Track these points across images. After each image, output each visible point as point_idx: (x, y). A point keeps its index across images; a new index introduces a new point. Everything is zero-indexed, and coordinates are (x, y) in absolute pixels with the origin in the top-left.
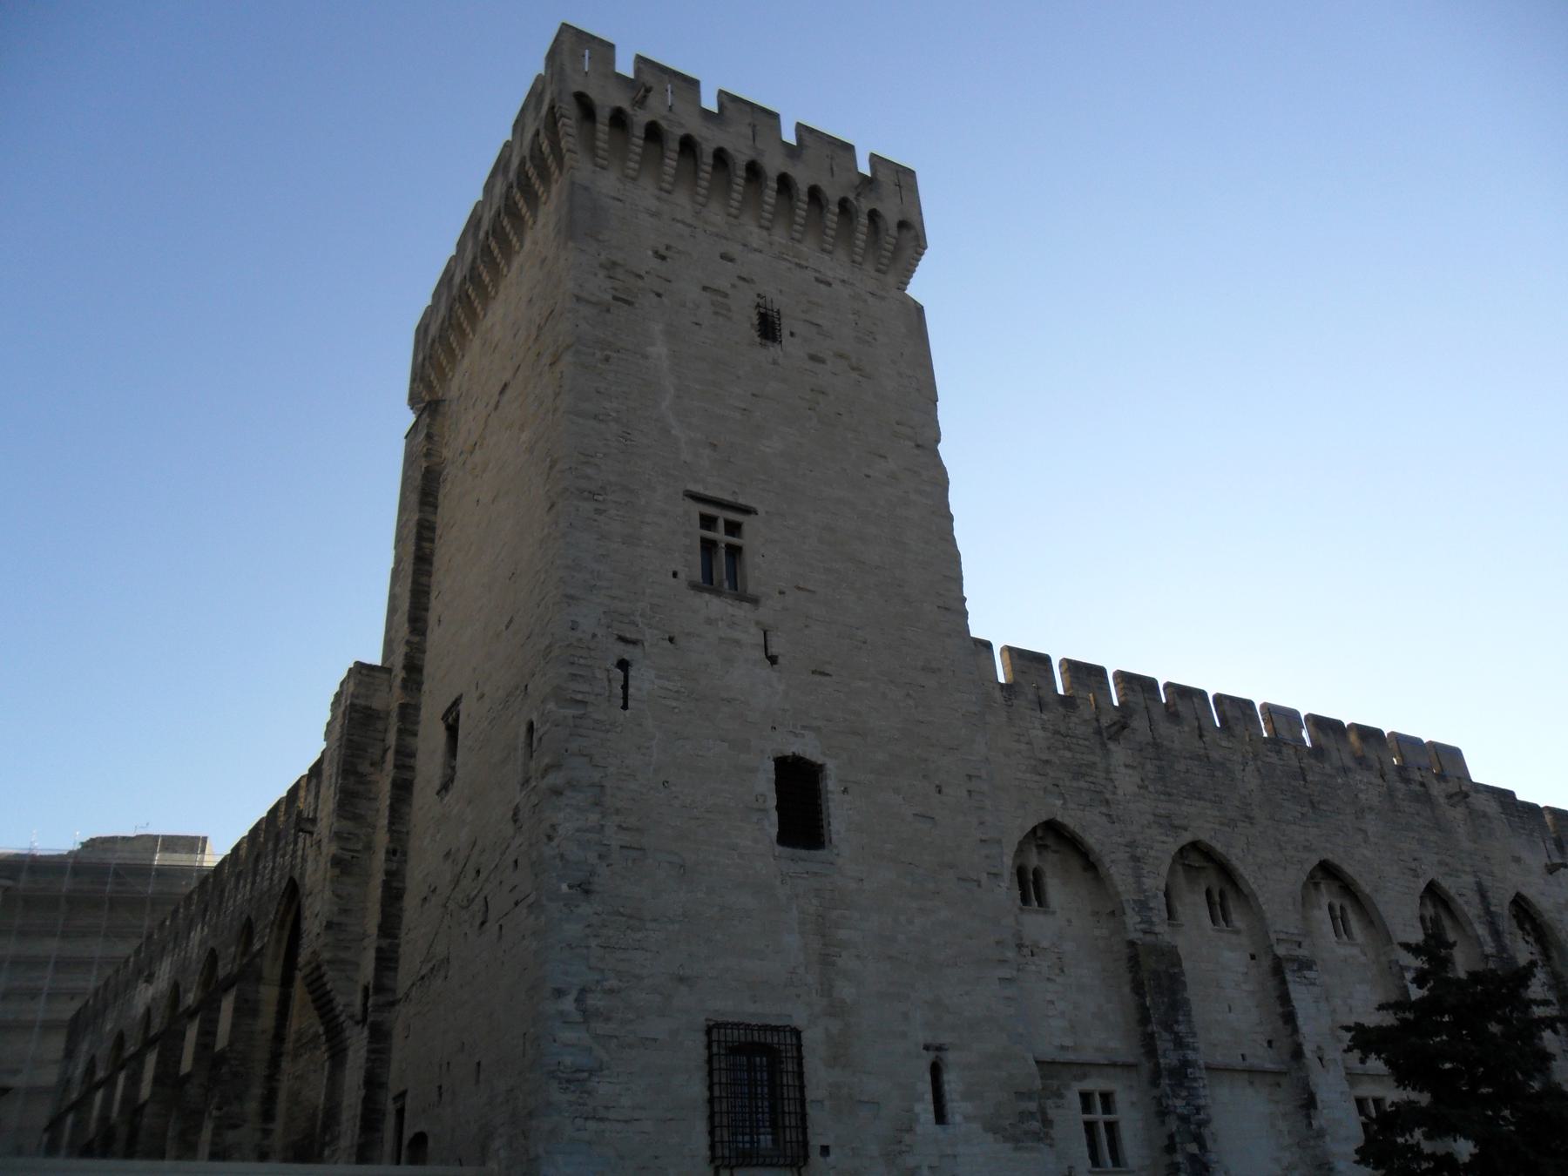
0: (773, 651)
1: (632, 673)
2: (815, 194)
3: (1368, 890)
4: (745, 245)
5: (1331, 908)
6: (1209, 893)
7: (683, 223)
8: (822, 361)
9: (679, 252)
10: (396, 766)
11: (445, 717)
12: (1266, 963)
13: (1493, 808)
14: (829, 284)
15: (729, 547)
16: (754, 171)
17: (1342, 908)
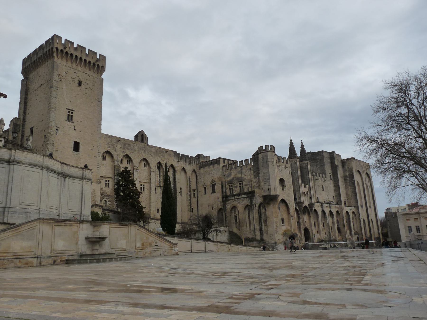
0: (75, 129)
1: (58, 131)
2: (90, 62)
3: (149, 162)
4: (78, 70)
5: (144, 164)
6: (128, 160)
7: (69, 67)
8: (87, 89)
9: (69, 72)
10: (22, 133)
11: (30, 129)
12: (133, 169)
13: (172, 153)
14: (90, 76)
15: (71, 115)
16: (81, 59)
17: (146, 164)
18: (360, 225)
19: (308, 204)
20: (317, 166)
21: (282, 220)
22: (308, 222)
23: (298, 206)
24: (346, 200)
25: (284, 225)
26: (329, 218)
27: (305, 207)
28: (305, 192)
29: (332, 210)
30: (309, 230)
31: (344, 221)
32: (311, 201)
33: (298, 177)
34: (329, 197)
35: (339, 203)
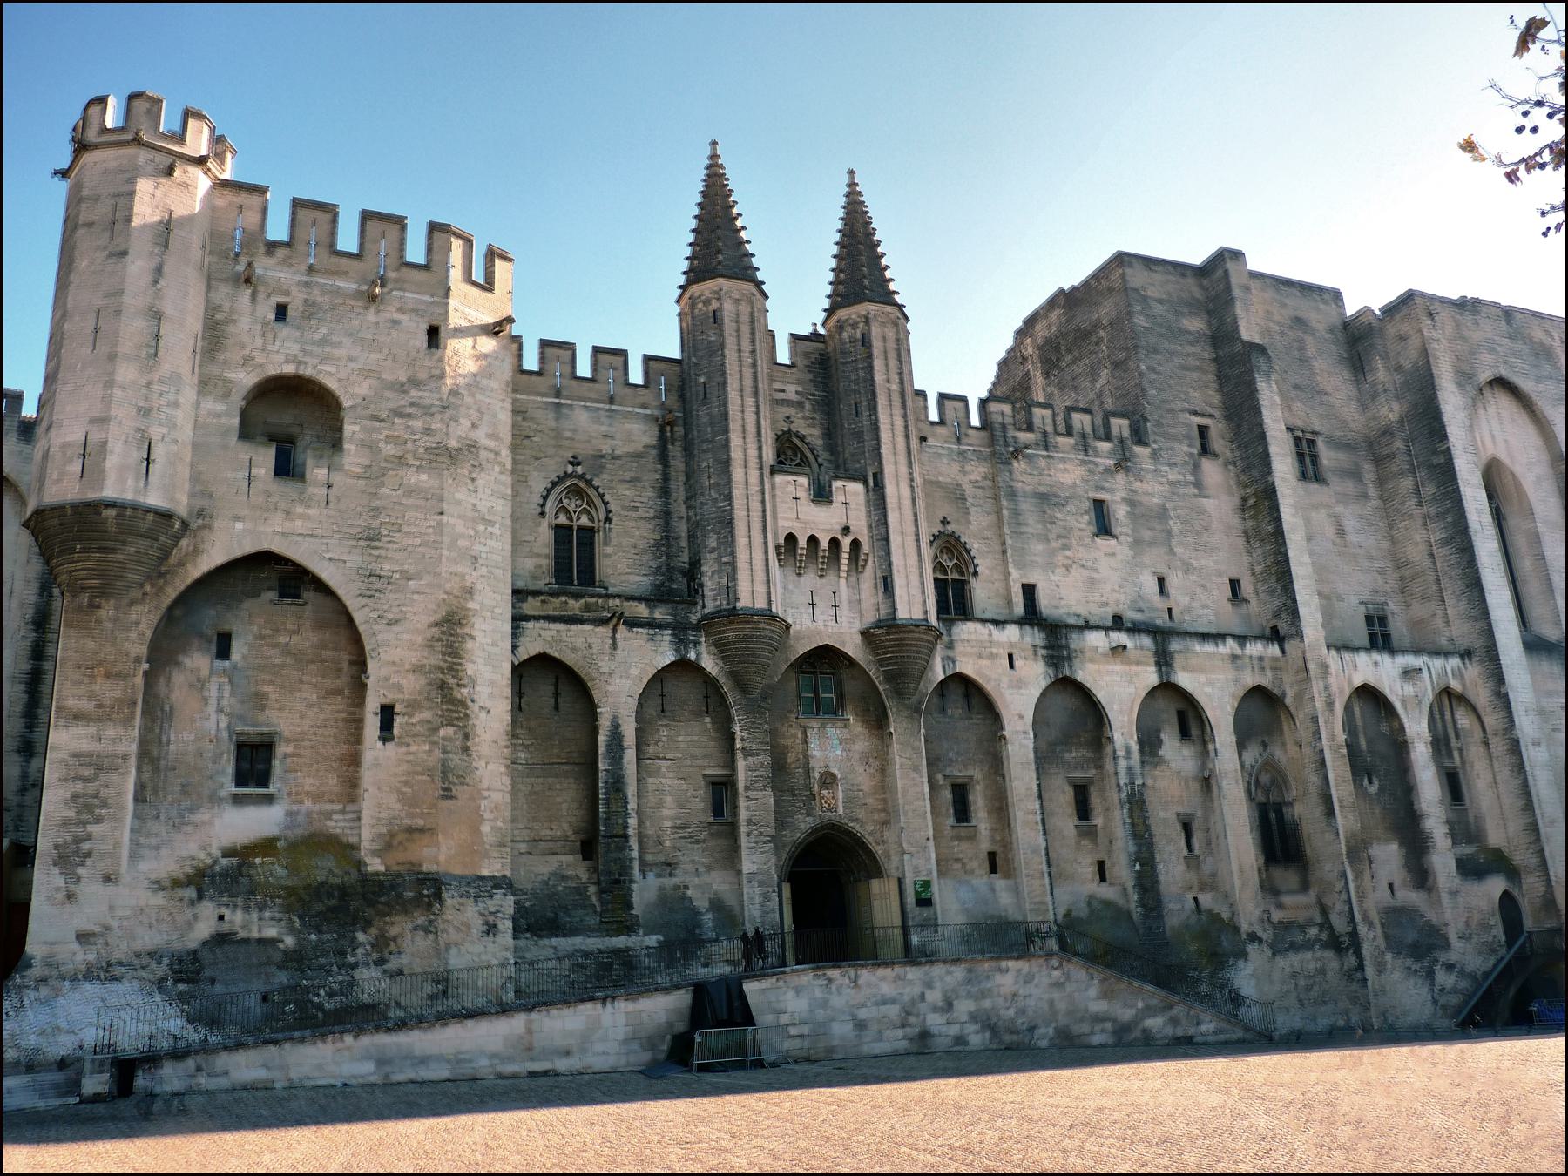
18: (1526, 792)
19: (866, 634)
20: (1093, 375)
21: (240, 747)
22: (864, 779)
23: (723, 650)
24: (1393, 607)
25: (269, 799)
26: (1149, 743)
27: (825, 658)
28: (813, 540)
29: (1184, 679)
30: (878, 850)
31: (1323, 763)
32: (884, 612)
33: (725, 416)
34: (1173, 582)
35: (1284, 627)
